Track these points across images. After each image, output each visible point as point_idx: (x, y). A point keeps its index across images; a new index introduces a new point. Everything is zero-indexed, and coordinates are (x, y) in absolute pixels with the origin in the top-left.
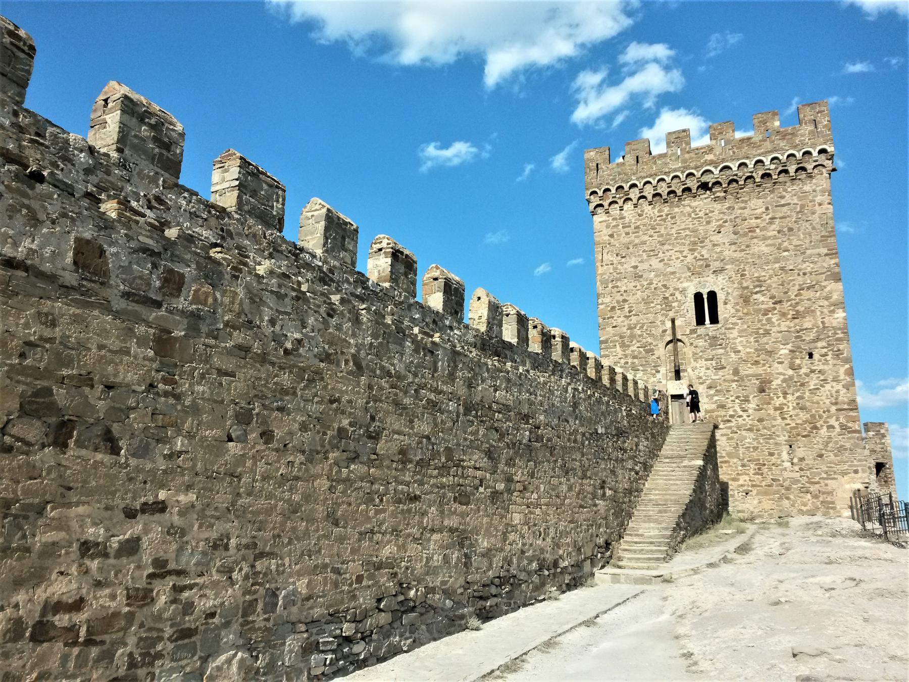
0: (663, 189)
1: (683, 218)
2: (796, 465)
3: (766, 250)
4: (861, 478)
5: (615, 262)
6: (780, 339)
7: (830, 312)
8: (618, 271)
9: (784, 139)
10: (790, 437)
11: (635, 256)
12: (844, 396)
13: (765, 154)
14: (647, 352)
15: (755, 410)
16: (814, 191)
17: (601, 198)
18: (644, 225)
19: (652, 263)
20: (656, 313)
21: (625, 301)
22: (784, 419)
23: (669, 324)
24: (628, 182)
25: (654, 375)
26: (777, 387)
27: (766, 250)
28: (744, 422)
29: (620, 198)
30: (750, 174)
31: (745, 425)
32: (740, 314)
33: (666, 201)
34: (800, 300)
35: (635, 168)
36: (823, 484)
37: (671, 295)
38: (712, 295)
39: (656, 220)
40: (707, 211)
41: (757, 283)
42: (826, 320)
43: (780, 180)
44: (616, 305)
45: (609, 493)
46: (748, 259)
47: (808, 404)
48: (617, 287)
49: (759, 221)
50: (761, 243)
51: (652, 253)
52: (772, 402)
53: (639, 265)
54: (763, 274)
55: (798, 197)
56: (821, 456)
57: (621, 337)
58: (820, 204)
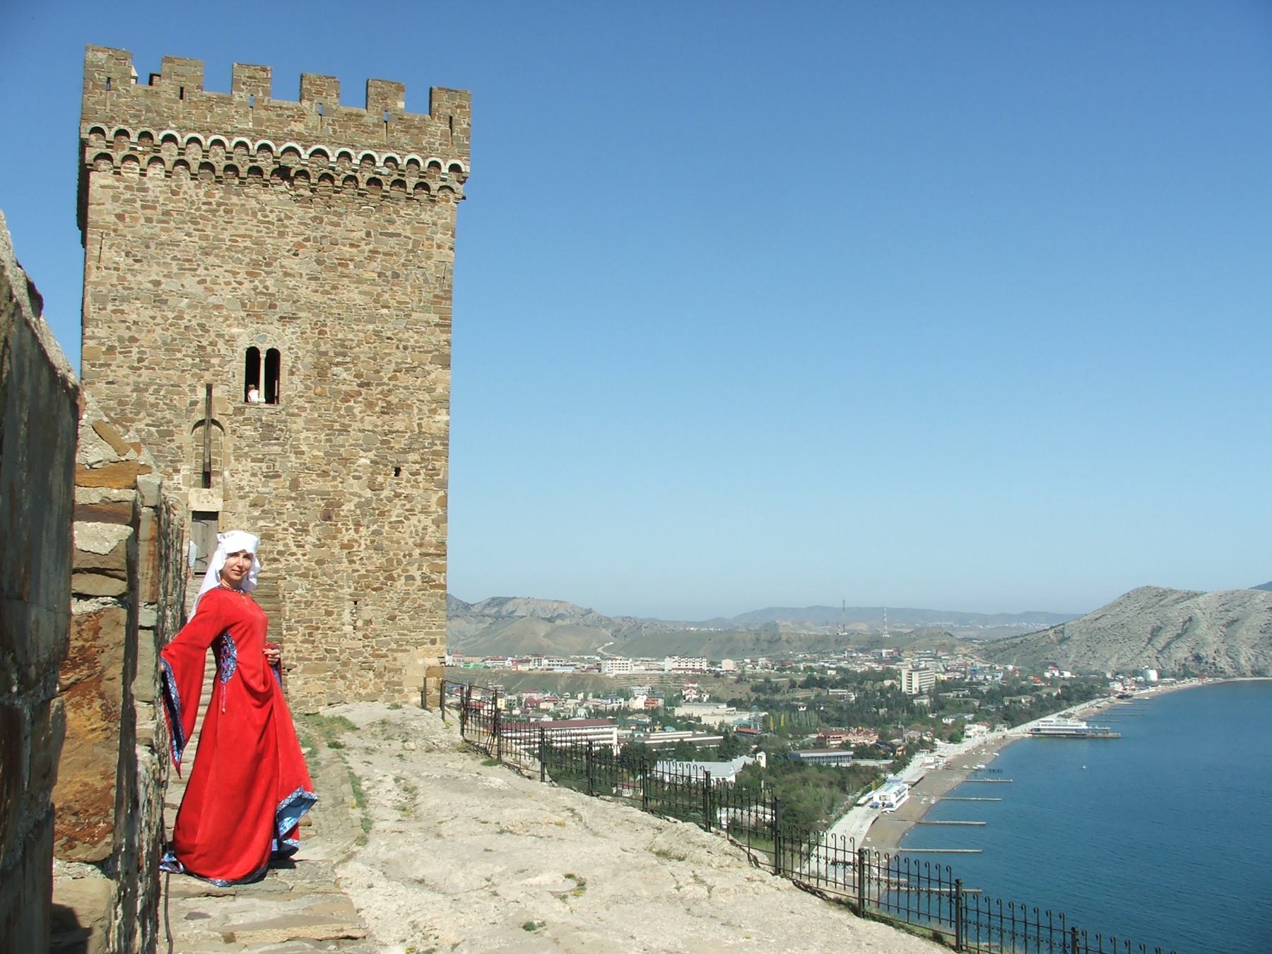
0: (218, 159)
1: (243, 216)
2: (360, 629)
3: (359, 299)
4: (438, 650)
5: (122, 266)
6: (361, 442)
7: (430, 411)
8: (126, 284)
9: (407, 132)
10: (356, 589)
11: (158, 264)
12: (432, 536)
13: (380, 147)
14: (163, 434)
16: (435, 224)
17: (110, 145)
18: (180, 213)
20: (183, 371)
21: (133, 340)
22: (351, 562)
23: (202, 393)
24: (162, 129)
25: (170, 477)
26: (348, 514)
27: (359, 299)
28: (297, 563)
29: (144, 153)
30: (353, 174)
31: (298, 568)
33: (219, 181)
34: (394, 386)
36: (390, 658)
37: (211, 344)
38: (273, 356)
39: (199, 209)
40: (282, 215)
41: (340, 349)
42: (424, 422)
43: (393, 194)
44: (117, 344)
46: (332, 307)
47: (385, 543)
48: (122, 312)
49: (354, 250)
51: (187, 265)
52: (339, 535)
53: (163, 280)
54: (350, 336)
55: (413, 228)
56: (393, 618)
57: (121, 403)
58: (439, 247)
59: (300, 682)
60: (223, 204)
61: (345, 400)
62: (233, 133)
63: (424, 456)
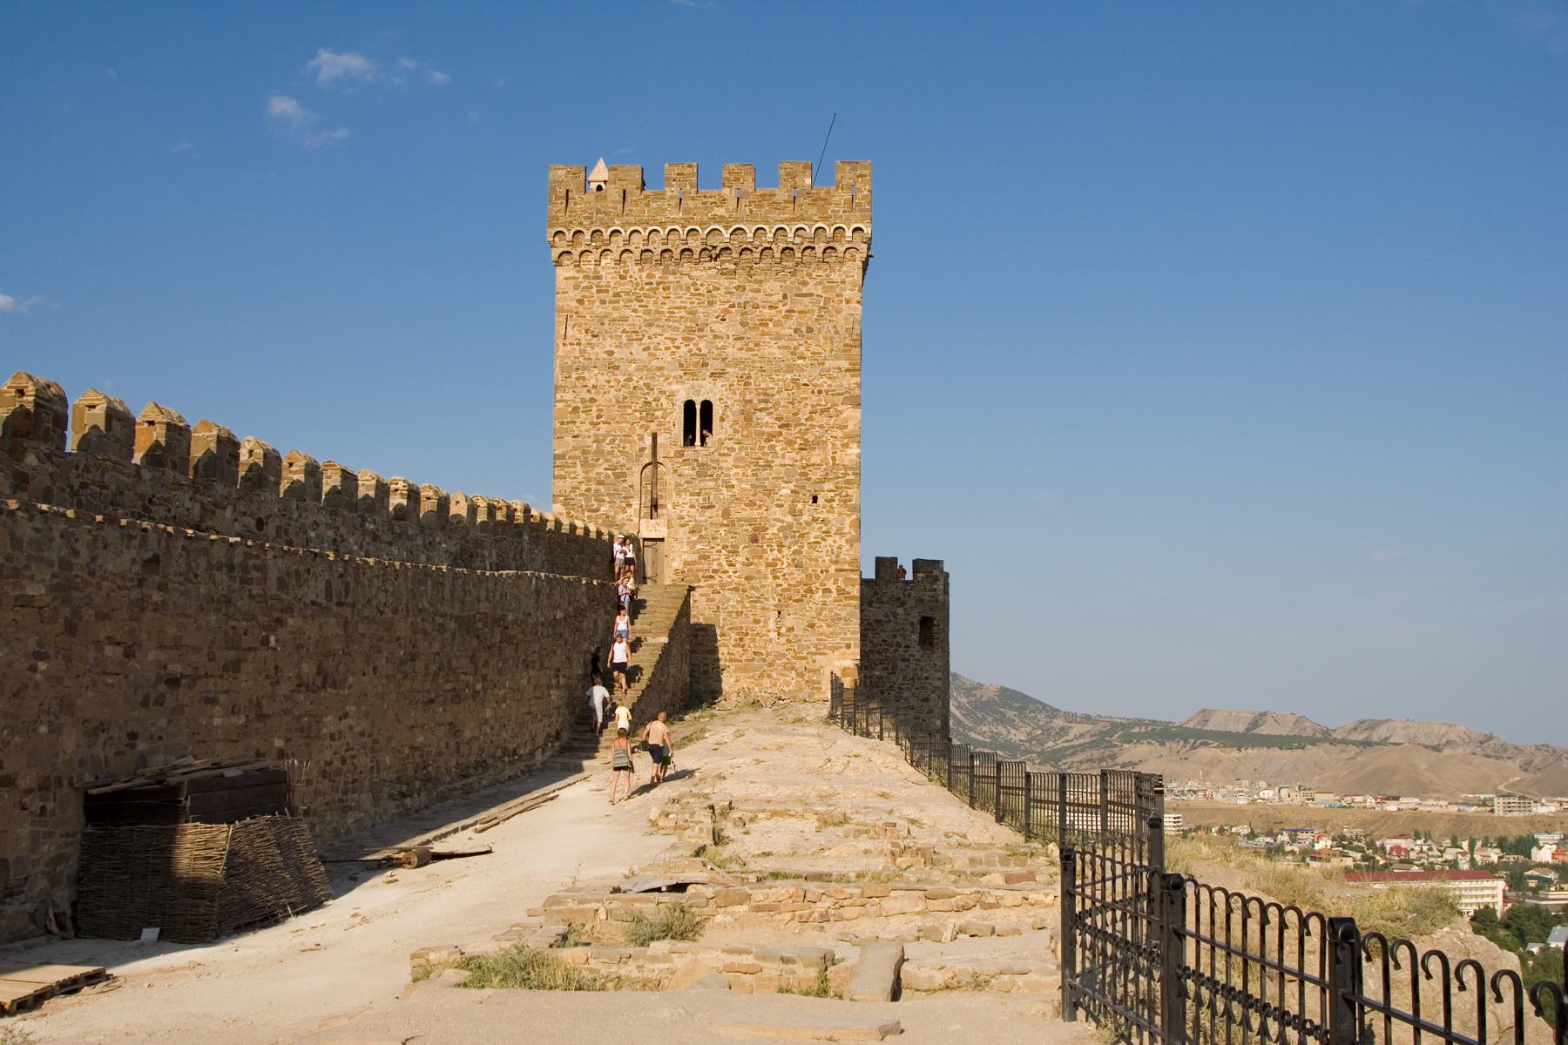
0: (657, 248)
1: (679, 291)
3: (778, 353)
4: (853, 653)
5: (583, 341)
7: (843, 445)
8: (586, 356)
14: (617, 476)
15: (744, 564)
19: (633, 351)
20: (633, 423)
21: (593, 400)
22: (775, 578)
23: (648, 441)
27: (778, 353)
30: (768, 245)
31: (730, 583)
32: (738, 436)
35: (620, 206)
36: (810, 660)
37: (655, 400)
38: (707, 406)
39: (643, 289)
40: (711, 288)
41: (763, 397)
45: (562, 681)
48: (584, 378)
49: (773, 311)
50: (773, 342)
51: (634, 336)
52: (765, 555)
53: (615, 350)
54: (772, 385)
56: (812, 626)
57: (584, 452)
58: (848, 302)
59: (732, 680)
60: (662, 283)
61: (768, 440)
62: (665, 223)
63: (840, 485)
